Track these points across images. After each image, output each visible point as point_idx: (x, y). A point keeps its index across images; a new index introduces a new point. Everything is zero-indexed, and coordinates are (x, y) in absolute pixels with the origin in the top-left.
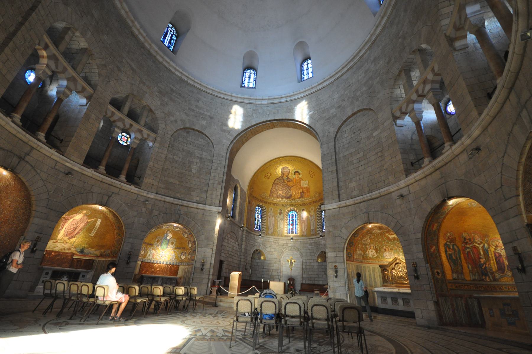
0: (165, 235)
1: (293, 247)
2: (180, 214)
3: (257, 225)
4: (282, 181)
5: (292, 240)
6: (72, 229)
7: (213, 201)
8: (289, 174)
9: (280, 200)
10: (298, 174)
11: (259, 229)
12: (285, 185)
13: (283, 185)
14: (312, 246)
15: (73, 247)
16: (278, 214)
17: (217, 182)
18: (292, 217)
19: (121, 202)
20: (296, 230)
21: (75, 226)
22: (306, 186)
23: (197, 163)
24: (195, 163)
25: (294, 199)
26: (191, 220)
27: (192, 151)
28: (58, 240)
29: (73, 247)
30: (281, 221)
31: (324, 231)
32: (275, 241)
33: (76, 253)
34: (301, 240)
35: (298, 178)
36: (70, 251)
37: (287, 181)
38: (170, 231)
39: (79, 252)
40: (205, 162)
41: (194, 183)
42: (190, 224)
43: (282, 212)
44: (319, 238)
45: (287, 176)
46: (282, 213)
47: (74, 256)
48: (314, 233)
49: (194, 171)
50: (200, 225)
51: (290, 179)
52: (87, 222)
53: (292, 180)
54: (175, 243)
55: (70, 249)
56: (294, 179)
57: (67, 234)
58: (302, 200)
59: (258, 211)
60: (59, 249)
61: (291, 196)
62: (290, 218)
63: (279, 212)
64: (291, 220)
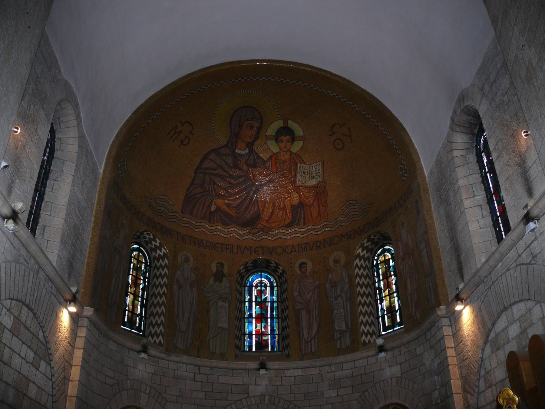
1: (267, 398)
3: (133, 312)
4: (230, 161)
5: (263, 372)
8: (256, 138)
9: (220, 231)
10: (287, 138)
11: (138, 329)
12: (238, 177)
13: (231, 177)
14: (342, 392)
16: (212, 280)
18: (260, 293)
20: (272, 338)
22: (314, 182)
25: (266, 230)
30: (220, 303)
31: (383, 333)
32: (198, 377)
34: (299, 372)
35: (287, 156)
37: (247, 164)
43: (226, 271)
44: (372, 360)
45: (250, 145)
46: (224, 275)
48: (348, 343)
51: (259, 157)
53: (265, 162)
56: (271, 157)
58: (296, 232)
59: (139, 261)
61: (257, 218)
62: (251, 295)
63: (214, 270)
64: (257, 303)
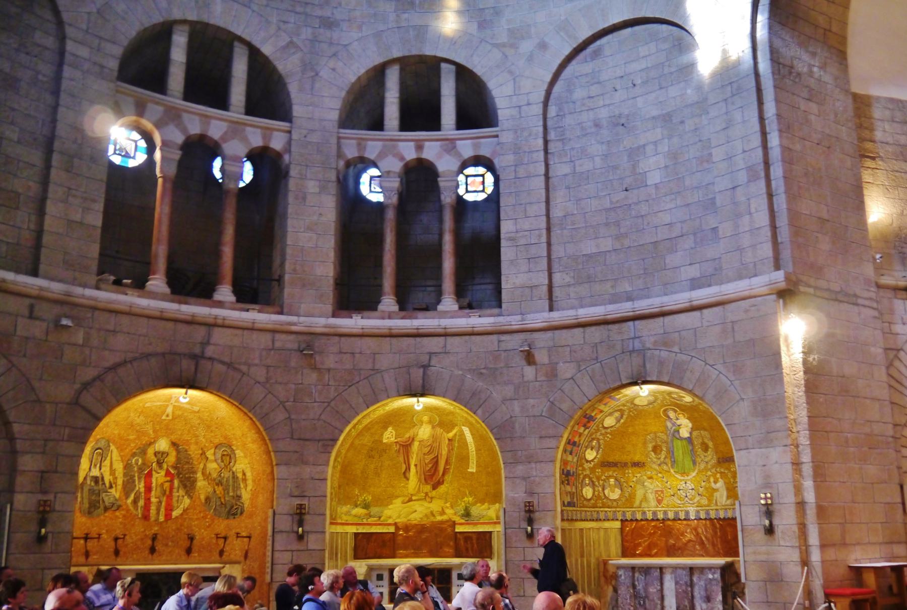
0: (669, 424)
2: (642, 352)
6: (429, 463)
7: (749, 257)
15: (447, 507)
17: (742, 177)
19: (460, 372)
21: (432, 456)
23: (655, 143)
24: (650, 149)
26: (684, 357)
27: (626, 112)
28: (412, 495)
29: (447, 507)
33: (457, 519)
36: (445, 518)
38: (675, 411)
39: (463, 516)
40: (682, 122)
41: (666, 218)
42: (688, 374)
47: (457, 527)
49: (654, 178)
50: (720, 367)
52: (449, 440)
54: (711, 444)
55: (443, 513)
57: (425, 479)
60: (421, 516)
